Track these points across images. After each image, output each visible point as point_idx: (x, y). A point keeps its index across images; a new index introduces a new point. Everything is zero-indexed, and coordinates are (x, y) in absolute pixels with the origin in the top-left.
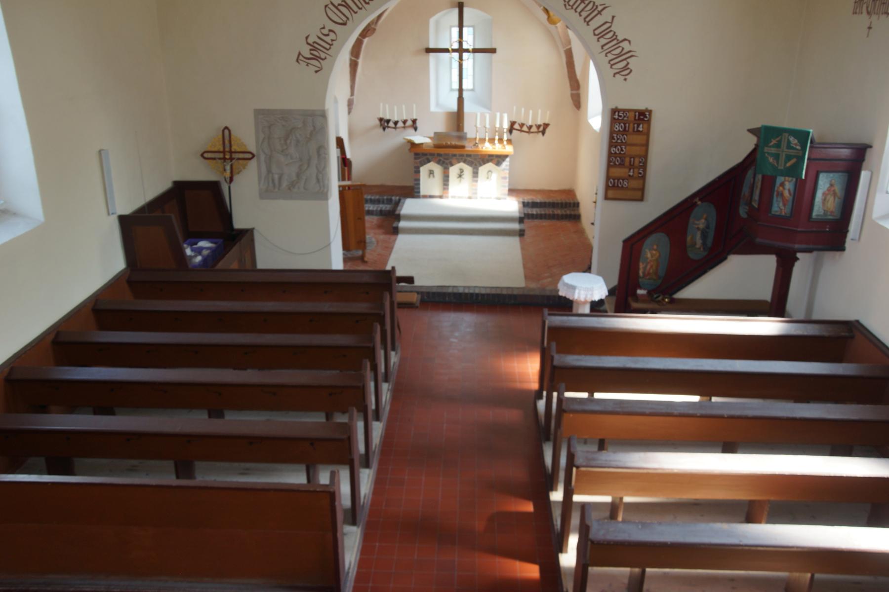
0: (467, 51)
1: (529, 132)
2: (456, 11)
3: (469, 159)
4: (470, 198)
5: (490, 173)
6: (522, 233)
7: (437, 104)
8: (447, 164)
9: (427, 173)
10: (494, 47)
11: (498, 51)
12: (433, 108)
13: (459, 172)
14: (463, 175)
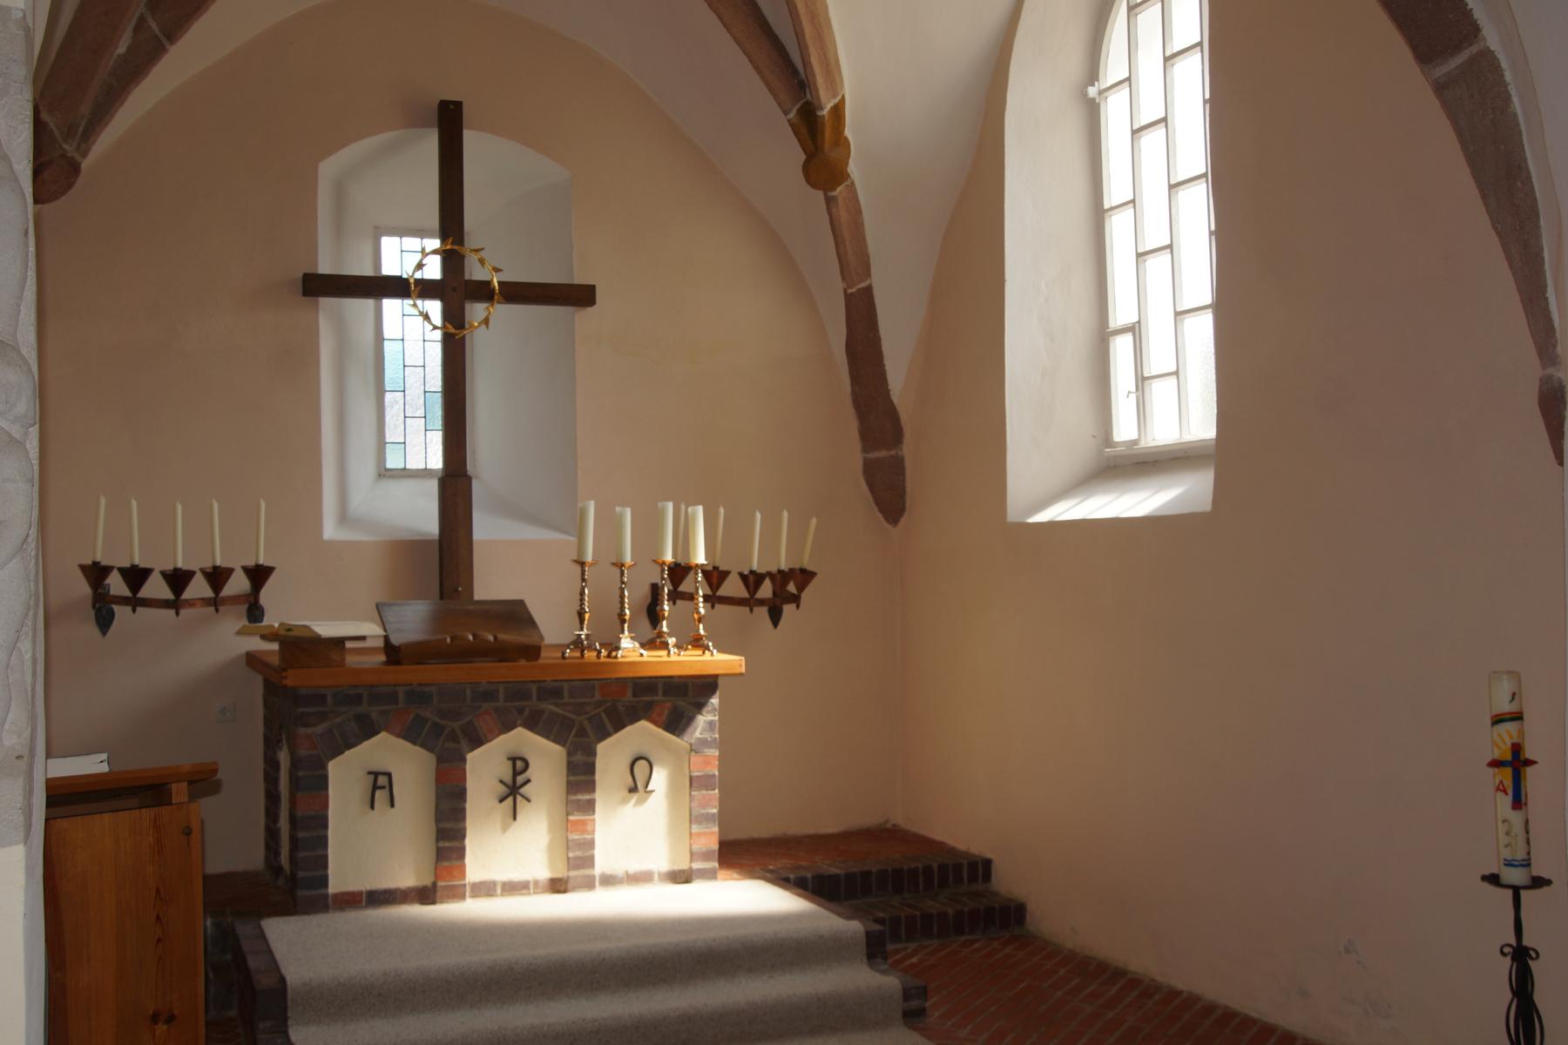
0: (483, 292)
1: (749, 602)
2: (429, 145)
3: (549, 707)
4: (557, 886)
5: (642, 764)
6: (915, 1004)
7: (344, 517)
8: (455, 739)
9: (360, 787)
10: (579, 279)
11: (600, 295)
12: (330, 530)
13: (505, 771)
14: (528, 781)
